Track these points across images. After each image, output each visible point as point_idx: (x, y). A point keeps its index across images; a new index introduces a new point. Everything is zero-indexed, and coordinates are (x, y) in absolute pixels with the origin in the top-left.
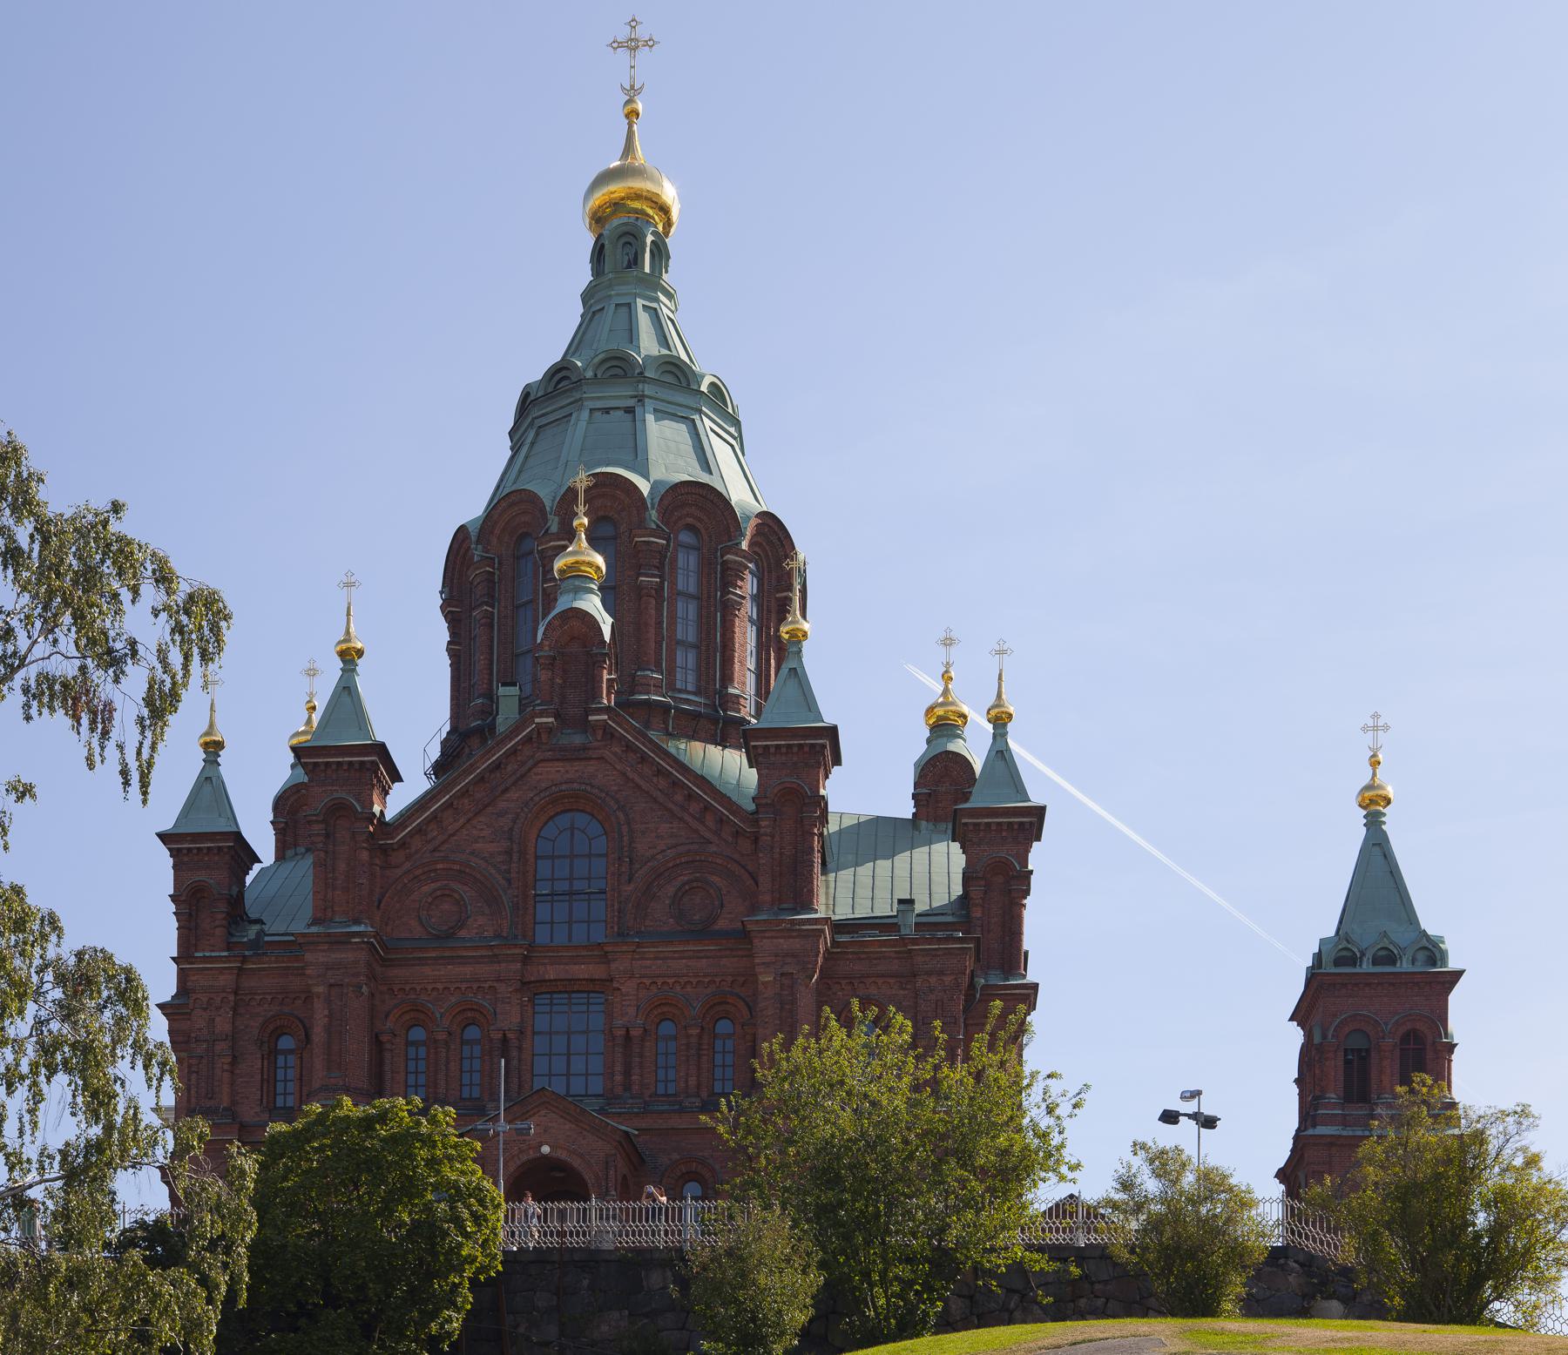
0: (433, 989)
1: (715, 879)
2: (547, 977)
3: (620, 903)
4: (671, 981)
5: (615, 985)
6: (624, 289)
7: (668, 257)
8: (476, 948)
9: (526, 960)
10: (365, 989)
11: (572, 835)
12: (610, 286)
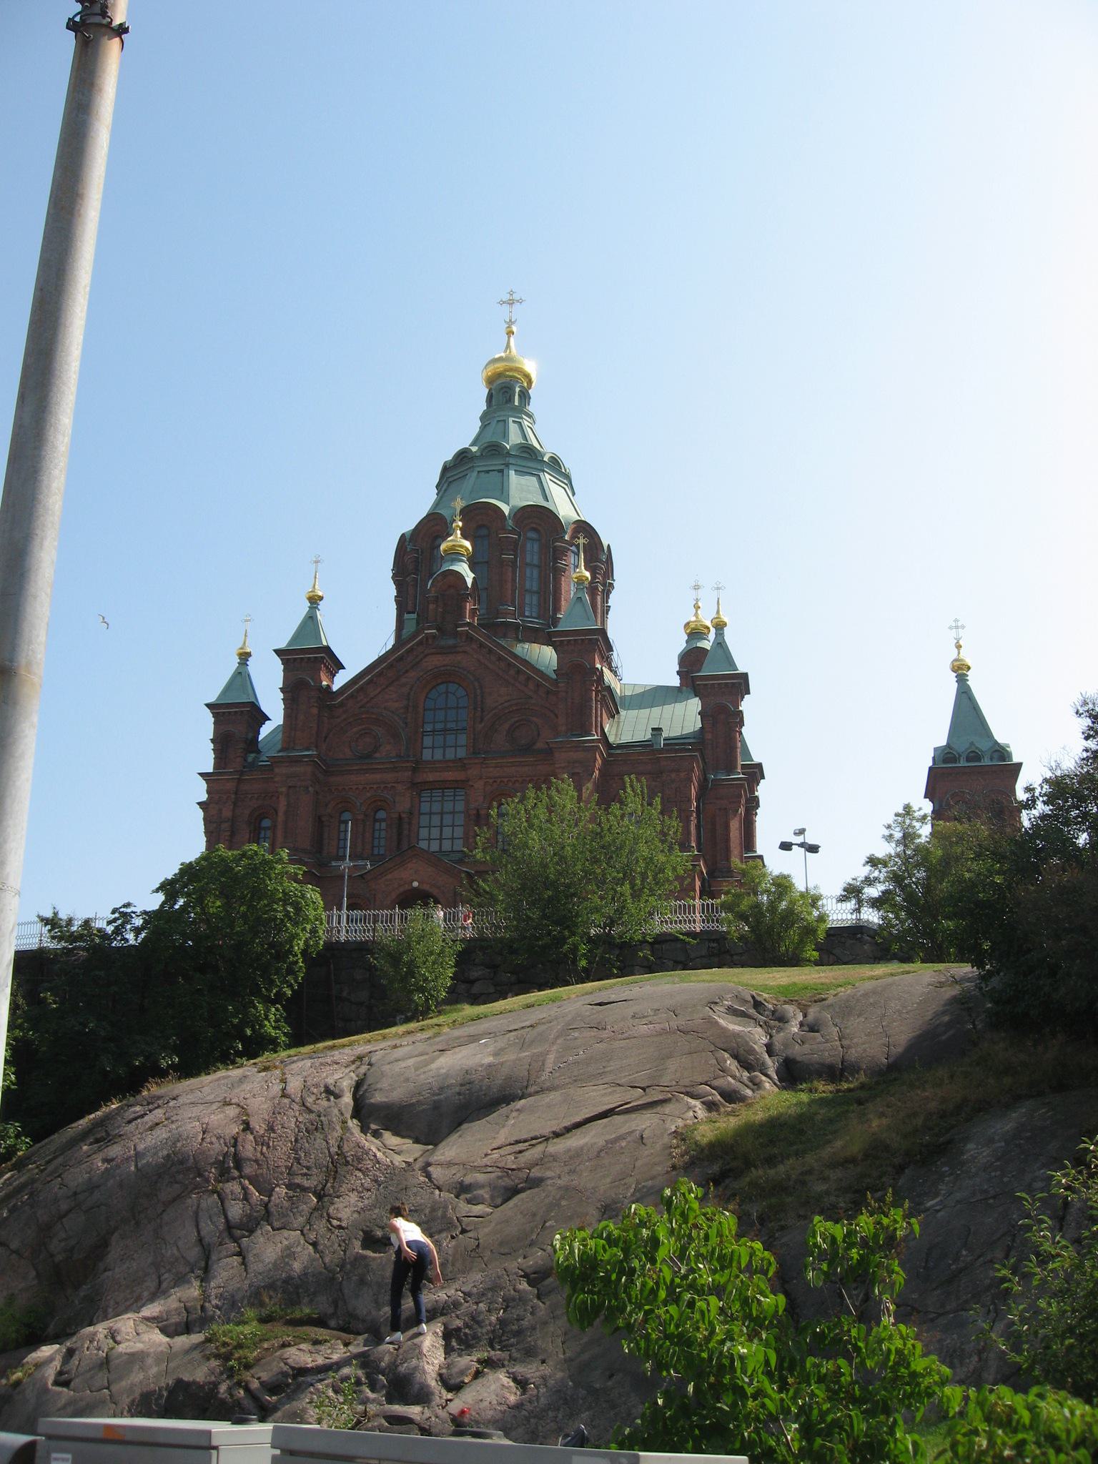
0: (357, 788)
1: (534, 719)
2: (428, 780)
3: (474, 735)
4: (506, 780)
5: (471, 783)
6: (502, 413)
7: (530, 398)
8: (383, 763)
9: (414, 770)
10: (310, 789)
11: (447, 696)
12: (495, 413)
